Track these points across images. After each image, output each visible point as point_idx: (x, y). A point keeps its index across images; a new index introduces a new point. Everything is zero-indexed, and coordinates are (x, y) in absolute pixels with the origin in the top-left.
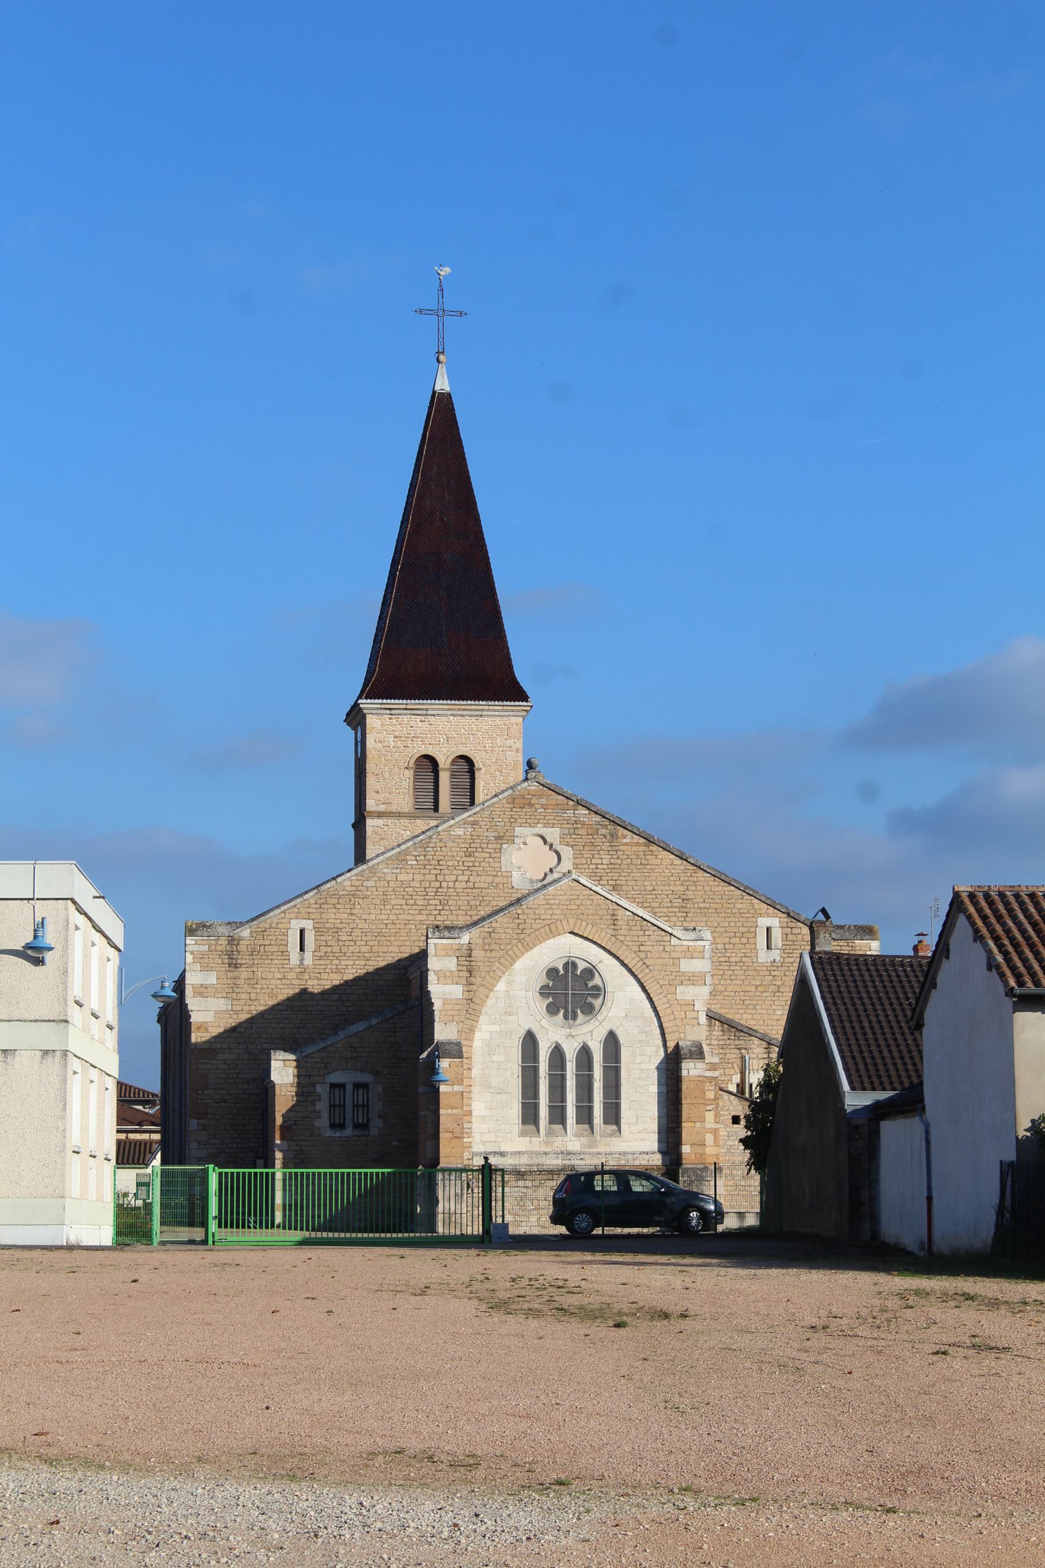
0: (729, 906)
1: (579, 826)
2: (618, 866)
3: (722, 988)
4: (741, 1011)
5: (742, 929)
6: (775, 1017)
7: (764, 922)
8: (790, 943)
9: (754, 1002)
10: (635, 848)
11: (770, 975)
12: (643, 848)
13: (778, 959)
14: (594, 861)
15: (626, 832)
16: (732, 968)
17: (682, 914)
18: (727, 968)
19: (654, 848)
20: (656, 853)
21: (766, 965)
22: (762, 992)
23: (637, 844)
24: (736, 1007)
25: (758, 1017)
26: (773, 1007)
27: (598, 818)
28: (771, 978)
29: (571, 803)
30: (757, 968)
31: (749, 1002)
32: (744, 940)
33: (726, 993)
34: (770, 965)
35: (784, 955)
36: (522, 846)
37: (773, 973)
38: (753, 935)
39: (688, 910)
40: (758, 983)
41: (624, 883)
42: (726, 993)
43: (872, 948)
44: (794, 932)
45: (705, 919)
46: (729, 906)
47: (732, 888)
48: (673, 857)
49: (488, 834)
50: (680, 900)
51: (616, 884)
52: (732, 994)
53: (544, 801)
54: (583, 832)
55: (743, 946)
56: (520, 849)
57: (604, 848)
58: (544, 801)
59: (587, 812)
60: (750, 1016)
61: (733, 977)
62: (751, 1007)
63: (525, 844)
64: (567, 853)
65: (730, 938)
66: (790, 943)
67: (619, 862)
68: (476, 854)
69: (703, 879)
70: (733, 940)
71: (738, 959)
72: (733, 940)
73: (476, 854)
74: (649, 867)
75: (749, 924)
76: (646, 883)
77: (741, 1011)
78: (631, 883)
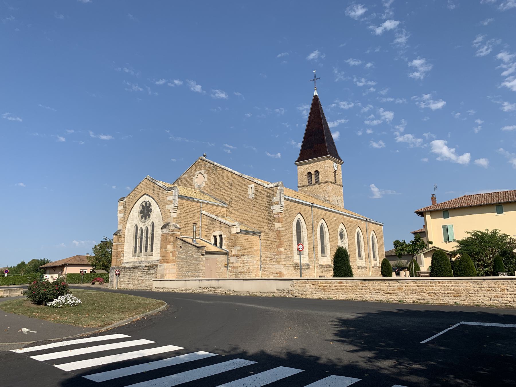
0: (241, 183)
1: (209, 168)
2: (216, 177)
3: (240, 208)
4: (245, 214)
5: (245, 189)
6: (253, 215)
7: (250, 186)
8: (257, 191)
9: (248, 211)
10: (220, 172)
11: (252, 202)
12: (222, 171)
13: (254, 196)
14: (212, 177)
15: (218, 168)
16: (242, 201)
17: (230, 188)
18: (241, 201)
19: (224, 170)
20: (225, 172)
21: (251, 199)
22: (250, 207)
23: (221, 170)
24: (243, 213)
25: (249, 215)
26: (253, 212)
27: (212, 165)
28: (252, 203)
29: (207, 163)
30: (249, 200)
31: (247, 211)
32: (245, 192)
33: (241, 209)
34: (251, 199)
35: (255, 195)
36: (197, 176)
37: (252, 201)
38: (247, 190)
39: (232, 186)
40: (249, 205)
41: (218, 182)
42: (241, 209)
43: (278, 189)
44: (258, 187)
45: (236, 188)
46: (241, 183)
47: (242, 178)
48: (228, 172)
49: (190, 175)
50: (230, 184)
51: (216, 182)
52: (242, 209)
53: (201, 163)
54: (209, 170)
55: (245, 194)
56: (197, 178)
57: (214, 173)
58: (201, 163)
59: (210, 164)
60: (247, 215)
61: (243, 204)
62: (247, 212)
63: (198, 176)
64: (206, 176)
65: (242, 192)
66: (257, 191)
67: (217, 176)
68: (188, 181)
69: (235, 177)
70: (243, 193)
71: (244, 198)
72: (243, 193)
73: (188, 181)
74: (223, 176)
75: (246, 187)
76: (223, 181)
77: (245, 214)
78: (219, 181)
